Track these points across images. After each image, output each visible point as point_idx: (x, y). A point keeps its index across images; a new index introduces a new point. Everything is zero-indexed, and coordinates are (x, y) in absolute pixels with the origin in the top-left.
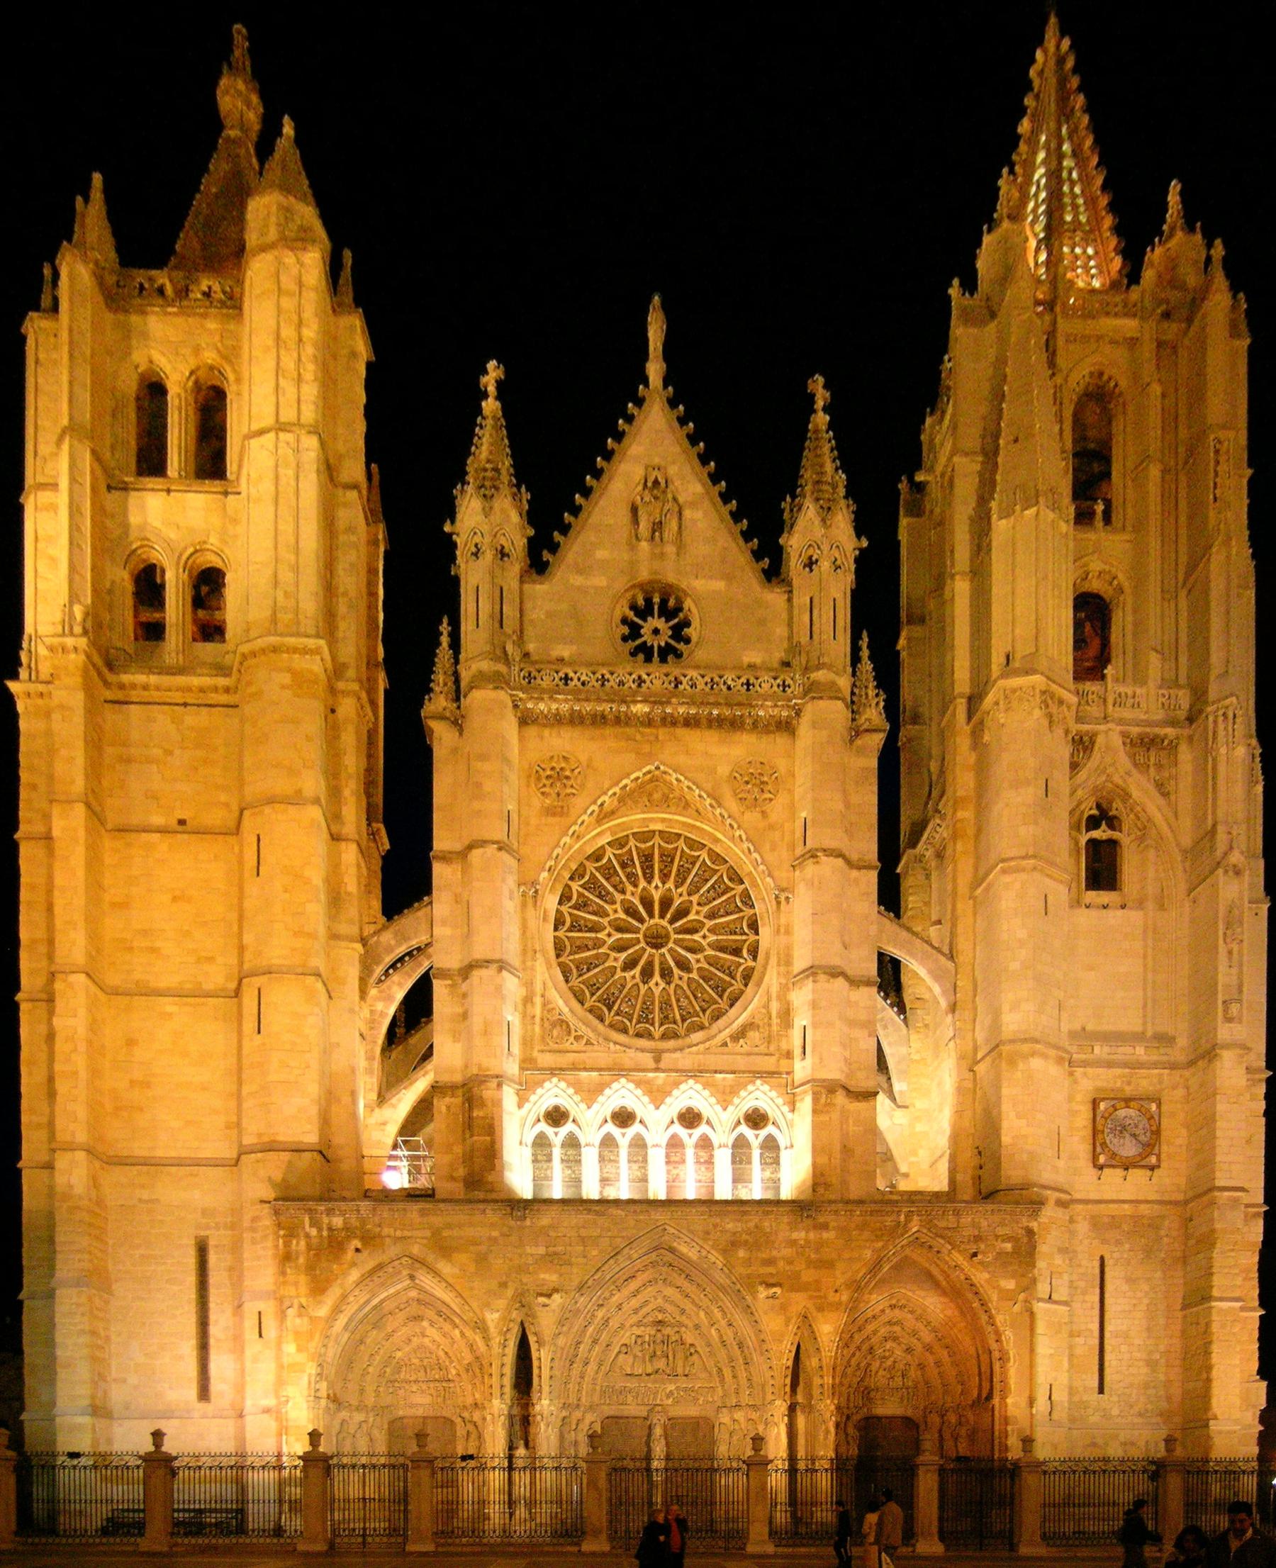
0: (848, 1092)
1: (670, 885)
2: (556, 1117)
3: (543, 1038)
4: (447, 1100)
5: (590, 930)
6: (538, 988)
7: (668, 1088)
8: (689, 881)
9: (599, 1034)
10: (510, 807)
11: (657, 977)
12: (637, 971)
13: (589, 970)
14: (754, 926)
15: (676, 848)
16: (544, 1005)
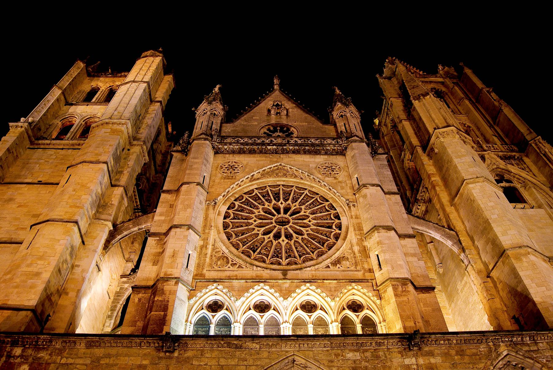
0: (416, 288)
1: (289, 202)
2: (215, 307)
3: (211, 265)
4: (141, 295)
5: (245, 219)
6: (211, 241)
7: (293, 289)
8: (299, 201)
9: (247, 262)
10: (205, 174)
11: (283, 237)
12: (272, 235)
13: (242, 235)
14: (338, 217)
15: (291, 190)
16: (213, 249)
